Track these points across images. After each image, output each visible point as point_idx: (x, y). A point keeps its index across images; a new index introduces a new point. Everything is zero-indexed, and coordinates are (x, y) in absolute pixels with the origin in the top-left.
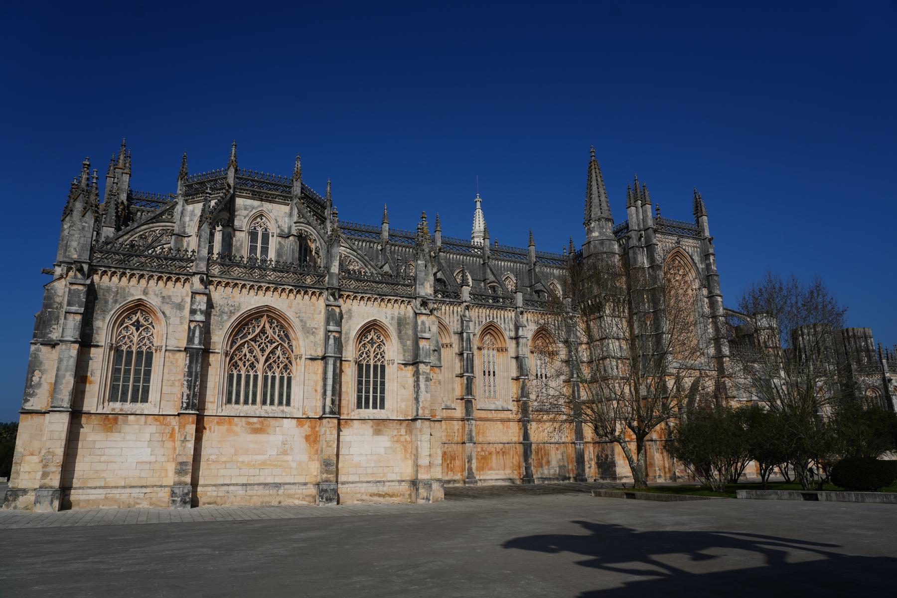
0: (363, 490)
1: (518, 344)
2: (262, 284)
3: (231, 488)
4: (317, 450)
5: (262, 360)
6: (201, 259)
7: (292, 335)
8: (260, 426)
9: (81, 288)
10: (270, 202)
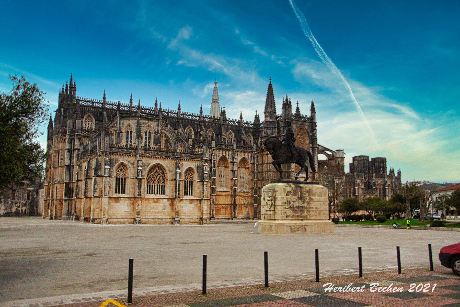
5: (157, 180)
6: (140, 149)
7: (165, 172)
8: (157, 201)
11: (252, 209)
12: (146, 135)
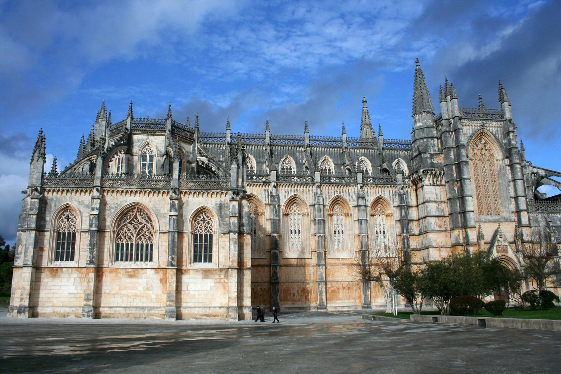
0: (196, 312)
1: (359, 210)
2: (133, 190)
3: (118, 309)
6: (98, 178)
7: (152, 219)
8: (133, 274)
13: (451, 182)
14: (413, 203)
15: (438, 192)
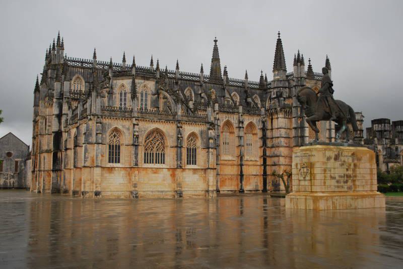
0: (190, 193)
1: (239, 130)
4: (174, 180)
9: (99, 124)
10: (147, 80)
11: (261, 180)
12: (142, 96)
13: (296, 118)
14: (269, 127)
15: (286, 122)
